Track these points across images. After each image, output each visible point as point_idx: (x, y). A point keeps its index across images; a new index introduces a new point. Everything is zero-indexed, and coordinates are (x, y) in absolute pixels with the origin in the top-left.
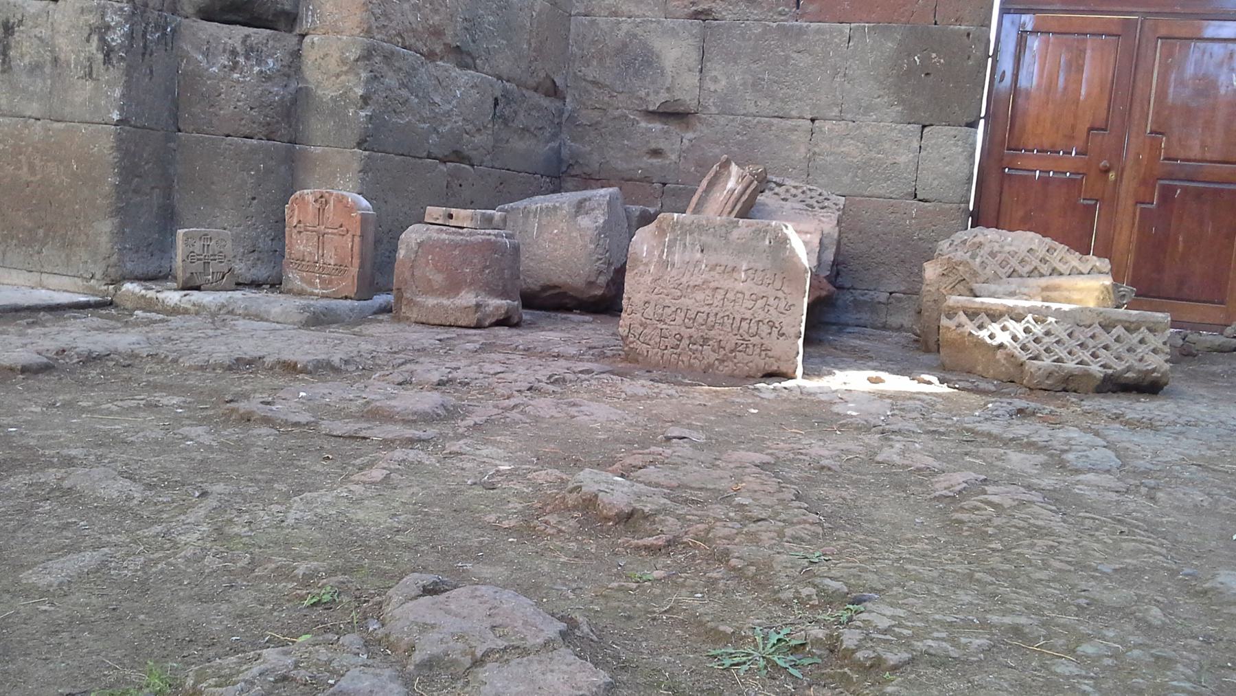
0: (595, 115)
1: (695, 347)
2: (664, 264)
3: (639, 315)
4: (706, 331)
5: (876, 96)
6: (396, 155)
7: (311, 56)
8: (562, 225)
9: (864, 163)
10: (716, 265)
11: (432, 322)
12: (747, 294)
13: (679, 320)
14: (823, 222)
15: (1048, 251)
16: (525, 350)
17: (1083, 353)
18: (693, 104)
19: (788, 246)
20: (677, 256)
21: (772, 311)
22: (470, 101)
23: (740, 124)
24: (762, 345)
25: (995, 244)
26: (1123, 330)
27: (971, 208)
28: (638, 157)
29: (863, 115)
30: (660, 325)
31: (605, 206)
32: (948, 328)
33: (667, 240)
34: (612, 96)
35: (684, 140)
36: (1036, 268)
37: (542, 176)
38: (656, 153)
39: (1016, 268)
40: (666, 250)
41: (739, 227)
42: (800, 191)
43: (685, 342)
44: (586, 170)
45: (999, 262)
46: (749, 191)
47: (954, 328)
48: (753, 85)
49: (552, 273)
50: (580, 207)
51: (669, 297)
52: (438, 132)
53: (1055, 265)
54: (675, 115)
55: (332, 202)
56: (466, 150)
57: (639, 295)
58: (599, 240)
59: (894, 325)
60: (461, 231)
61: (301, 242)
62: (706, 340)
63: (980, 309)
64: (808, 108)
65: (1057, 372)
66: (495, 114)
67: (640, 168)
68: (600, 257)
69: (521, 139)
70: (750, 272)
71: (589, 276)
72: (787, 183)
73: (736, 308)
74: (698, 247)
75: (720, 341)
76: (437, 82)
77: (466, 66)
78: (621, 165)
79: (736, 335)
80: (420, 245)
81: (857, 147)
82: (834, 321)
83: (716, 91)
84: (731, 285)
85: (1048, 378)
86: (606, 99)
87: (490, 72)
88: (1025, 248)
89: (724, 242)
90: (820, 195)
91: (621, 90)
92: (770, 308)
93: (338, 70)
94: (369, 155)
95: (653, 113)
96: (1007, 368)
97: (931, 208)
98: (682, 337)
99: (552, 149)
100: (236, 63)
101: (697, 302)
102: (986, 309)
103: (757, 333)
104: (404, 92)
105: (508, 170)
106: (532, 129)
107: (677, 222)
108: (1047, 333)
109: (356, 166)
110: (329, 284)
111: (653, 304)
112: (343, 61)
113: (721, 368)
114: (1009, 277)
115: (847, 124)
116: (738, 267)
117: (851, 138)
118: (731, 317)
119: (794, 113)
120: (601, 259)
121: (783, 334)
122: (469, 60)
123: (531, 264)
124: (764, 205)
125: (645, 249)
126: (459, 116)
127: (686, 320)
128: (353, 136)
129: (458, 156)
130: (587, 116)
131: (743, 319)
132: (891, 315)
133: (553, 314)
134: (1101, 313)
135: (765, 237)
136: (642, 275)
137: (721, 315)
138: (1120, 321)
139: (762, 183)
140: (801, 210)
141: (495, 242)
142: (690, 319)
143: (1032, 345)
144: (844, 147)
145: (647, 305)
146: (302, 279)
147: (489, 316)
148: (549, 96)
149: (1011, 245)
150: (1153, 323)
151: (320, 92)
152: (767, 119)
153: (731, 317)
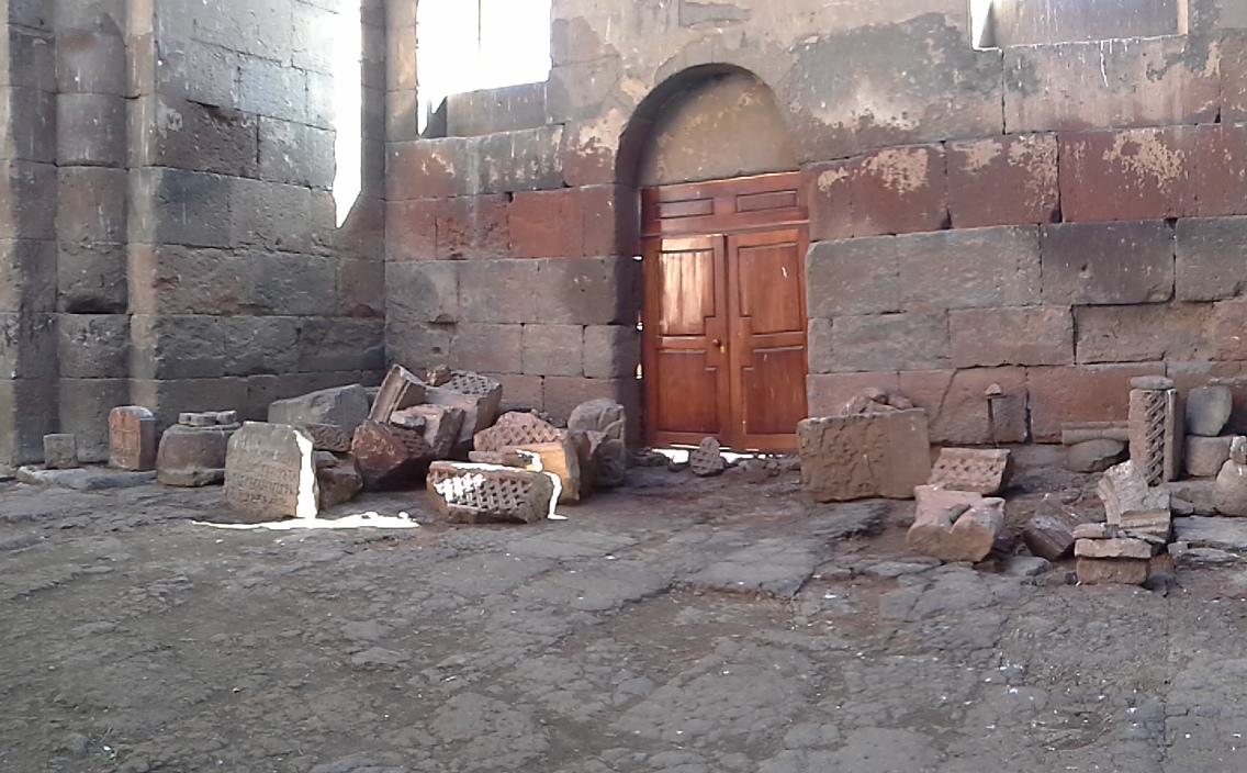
6: (193, 378)
7: (134, 326)
18: (455, 320)
48: (488, 302)
54: (445, 324)
56: (268, 367)
95: (434, 323)
100: (85, 337)
104: (197, 341)
109: (155, 390)
112: (147, 329)
119: (512, 320)
122: (266, 310)
128: (153, 372)
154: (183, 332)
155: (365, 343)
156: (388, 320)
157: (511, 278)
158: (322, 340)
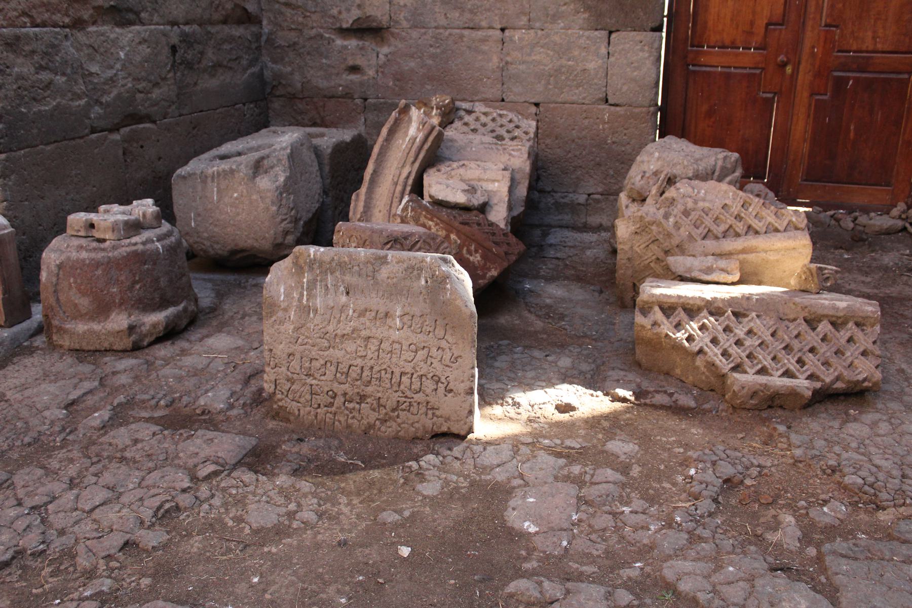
0: (293, 36)
1: (351, 405)
2: (305, 310)
3: (284, 369)
4: (363, 387)
5: (562, 3)
6: (47, 144)
8: (241, 188)
9: (556, 71)
10: (366, 310)
11: (86, 348)
12: (405, 344)
13: (330, 375)
14: (514, 156)
15: (743, 206)
16: (167, 406)
17: (788, 359)
19: (448, 286)
20: (318, 301)
21: (436, 364)
22: (138, 58)
23: (433, 37)
24: (428, 403)
25: (689, 199)
26: (830, 327)
27: (659, 103)
28: (338, 74)
29: (551, 23)
30: (310, 381)
31: (285, 162)
32: (643, 327)
33: (305, 280)
34: (305, 17)
35: (380, 56)
36: (731, 226)
37: (244, 104)
38: (355, 69)
39: (712, 228)
40: (305, 293)
41: (388, 263)
42: (490, 118)
43: (339, 400)
44: (290, 89)
45: (693, 222)
46: (431, 138)
47: (649, 327)
49: (237, 237)
50: (258, 167)
51: (316, 348)
52: (101, 103)
53: (750, 222)
56: (142, 110)
57: (281, 346)
58: (281, 200)
59: (593, 225)
60: (102, 246)
62: (363, 398)
63: (677, 303)
64: (497, 18)
65: (763, 392)
66: (174, 61)
67: (340, 85)
68: (284, 217)
69: (213, 76)
70: (406, 318)
71: (275, 238)
72: (476, 110)
73: (394, 360)
74: (342, 289)
75: (379, 398)
76: (91, 50)
77: (125, 23)
78: (323, 84)
79: (396, 391)
80: (60, 267)
81: (548, 55)
82: (537, 223)
83: (405, 6)
84: (385, 334)
85: (752, 397)
86: (300, 19)
87: (162, 22)
88: (718, 204)
89: (372, 282)
90: (511, 121)
91: (313, 10)
92: (433, 360)
94: (8, 157)
96: (707, 377)
97: (622, 113)
98: (336, 395)
99: (253, 74)
101: (347, 353)
102: (683, 303)
103: (420, 389)
104: (45, 76)
105: (201, 111)
106: (225, 63)
107: (315, 260)
108: (750, 332)
111: (298, 356)
113: (383, 429)
114: (704, 238)
115: (536, 33)
116: (392, 312)
117: (542, 47)
118: (389, 371)
119: (484, 24)
120: (285, 219)
121: (451, 391)
122: (131, 16)
123: (216, 230)
124: (452, 140)
125: (282, 290)
126: (127, 78)
127: (338, 375)
129: (135, 118)
130: (284, 38)
131: (402, 374)
132: (590, 215)
133: (242, 278)
134: (806, 307)
135: (419, 276)
136: (282, 322)
137: (376, 369)
138: (826, 316)
139: (449, 116)
140: (490, 144)
141: (143, 253)
142: (342, 374)
143: (734, 350)
144: (535, 55)
145: (291, 358)
147: (146, 336)
148: (243, 23)
149: (704, 200)
150: (862, 318)
152: (458, 31)
153: (389, 371)
154: (20, 60)
155: (244, 62)
156: (266, 28)
158: (199, 62)
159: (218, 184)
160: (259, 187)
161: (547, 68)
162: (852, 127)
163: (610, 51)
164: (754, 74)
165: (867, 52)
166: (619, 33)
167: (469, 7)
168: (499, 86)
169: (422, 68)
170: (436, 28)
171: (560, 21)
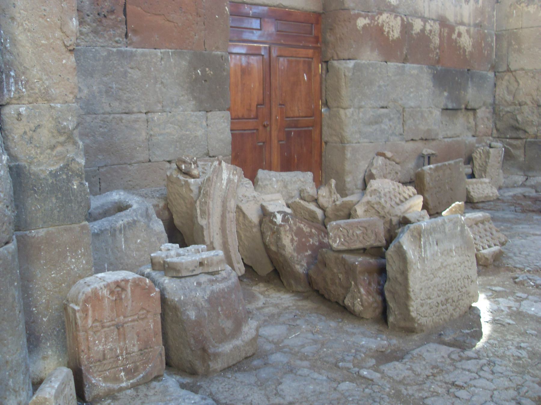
8: (142, 235)
29: (175, 108)
48: (107, 92)
55: (129, 290)
61: (100, 342)
64: (143, 106)
81: (175, 128)
83: (81, 98)
93: (53, 141)
110: (134, 372)
112: (61, 131)
115: (167, 114)
119: (135, 110)
146: (106, 379)
151: (34, 169)
157: (132, 68)
159: (124, 235)
160: (155, 231)
161: (175, 137)
162: (296, 157)
163: (208, 124)
164: (254, 133)
165: (297, 117)
166: (211, 112)
167: (125, 98)
168: (147, 152)
169: (94, 143)
170: (103, 114)
171: (180, 107)
